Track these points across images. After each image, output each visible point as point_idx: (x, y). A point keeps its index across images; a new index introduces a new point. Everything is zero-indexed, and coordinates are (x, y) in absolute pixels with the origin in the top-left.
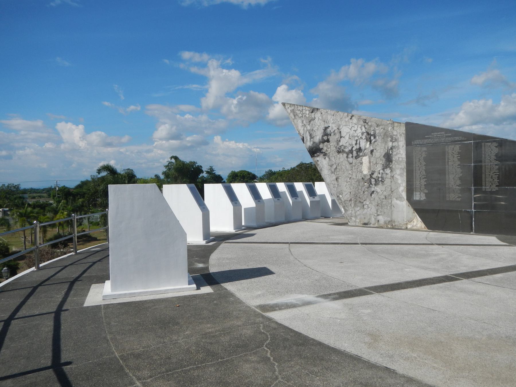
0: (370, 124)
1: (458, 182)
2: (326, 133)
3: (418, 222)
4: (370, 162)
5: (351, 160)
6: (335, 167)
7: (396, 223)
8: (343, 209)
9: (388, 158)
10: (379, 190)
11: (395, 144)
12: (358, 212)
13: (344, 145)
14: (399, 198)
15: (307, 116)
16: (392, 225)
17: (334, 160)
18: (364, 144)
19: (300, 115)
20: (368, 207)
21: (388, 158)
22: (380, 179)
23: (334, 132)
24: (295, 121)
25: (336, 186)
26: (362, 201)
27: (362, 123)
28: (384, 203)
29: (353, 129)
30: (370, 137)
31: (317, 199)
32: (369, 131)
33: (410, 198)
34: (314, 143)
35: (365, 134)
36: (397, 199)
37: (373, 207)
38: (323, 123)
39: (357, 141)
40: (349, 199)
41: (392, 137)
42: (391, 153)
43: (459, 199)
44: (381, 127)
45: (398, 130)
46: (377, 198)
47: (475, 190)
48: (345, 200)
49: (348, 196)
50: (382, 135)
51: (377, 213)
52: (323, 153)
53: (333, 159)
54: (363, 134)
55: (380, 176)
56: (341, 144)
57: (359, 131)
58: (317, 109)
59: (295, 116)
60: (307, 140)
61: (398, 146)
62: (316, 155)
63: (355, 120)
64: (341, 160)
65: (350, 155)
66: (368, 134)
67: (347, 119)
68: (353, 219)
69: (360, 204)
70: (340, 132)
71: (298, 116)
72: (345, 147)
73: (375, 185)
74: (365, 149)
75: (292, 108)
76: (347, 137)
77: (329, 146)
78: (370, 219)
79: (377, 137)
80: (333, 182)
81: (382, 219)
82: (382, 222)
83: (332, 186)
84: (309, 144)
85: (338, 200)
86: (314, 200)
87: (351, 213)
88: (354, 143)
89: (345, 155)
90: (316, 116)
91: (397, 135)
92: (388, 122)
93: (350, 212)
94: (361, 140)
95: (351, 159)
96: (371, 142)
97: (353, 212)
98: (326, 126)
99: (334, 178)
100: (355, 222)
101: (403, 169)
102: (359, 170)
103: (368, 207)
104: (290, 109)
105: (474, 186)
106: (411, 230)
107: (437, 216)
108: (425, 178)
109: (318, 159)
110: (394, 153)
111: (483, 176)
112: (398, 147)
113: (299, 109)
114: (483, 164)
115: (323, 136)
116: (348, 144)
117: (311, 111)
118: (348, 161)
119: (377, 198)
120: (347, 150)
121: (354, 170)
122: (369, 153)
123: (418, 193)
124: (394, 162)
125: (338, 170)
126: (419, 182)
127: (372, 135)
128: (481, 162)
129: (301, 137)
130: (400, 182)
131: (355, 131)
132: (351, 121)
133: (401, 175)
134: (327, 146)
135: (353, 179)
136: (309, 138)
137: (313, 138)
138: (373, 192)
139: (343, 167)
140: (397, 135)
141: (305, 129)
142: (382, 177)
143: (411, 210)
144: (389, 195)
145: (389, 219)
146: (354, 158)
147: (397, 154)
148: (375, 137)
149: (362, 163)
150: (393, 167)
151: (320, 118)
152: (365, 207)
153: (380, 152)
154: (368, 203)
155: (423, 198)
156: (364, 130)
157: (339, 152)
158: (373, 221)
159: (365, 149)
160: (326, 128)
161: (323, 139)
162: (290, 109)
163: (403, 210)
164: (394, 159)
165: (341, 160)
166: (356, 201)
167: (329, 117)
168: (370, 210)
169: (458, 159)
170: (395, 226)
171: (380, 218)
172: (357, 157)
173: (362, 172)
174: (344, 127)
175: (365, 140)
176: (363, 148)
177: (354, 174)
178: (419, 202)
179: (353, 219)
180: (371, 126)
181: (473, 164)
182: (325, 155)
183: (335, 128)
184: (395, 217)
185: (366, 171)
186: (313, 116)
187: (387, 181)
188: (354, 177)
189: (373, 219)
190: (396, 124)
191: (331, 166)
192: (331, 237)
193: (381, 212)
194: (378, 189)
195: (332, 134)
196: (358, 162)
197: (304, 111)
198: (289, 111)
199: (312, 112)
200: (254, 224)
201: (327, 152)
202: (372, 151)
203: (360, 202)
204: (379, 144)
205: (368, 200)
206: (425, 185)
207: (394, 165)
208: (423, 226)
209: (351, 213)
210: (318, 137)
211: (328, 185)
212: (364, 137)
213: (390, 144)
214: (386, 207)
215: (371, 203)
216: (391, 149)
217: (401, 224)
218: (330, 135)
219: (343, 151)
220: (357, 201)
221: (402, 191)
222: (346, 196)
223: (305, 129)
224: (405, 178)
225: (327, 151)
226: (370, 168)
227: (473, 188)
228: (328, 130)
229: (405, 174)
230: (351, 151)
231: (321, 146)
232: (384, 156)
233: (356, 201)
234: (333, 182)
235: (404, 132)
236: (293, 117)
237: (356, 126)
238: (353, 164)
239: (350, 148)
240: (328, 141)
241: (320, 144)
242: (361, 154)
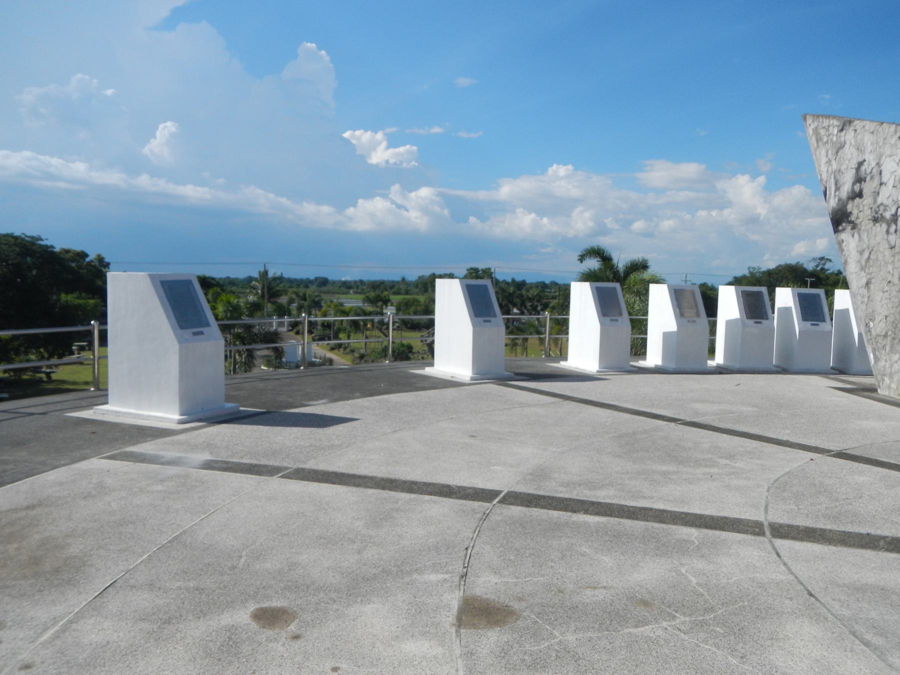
2: (859, 179)
6: (866, 255)
8: (871, 356)
13: (885, 202)
15: (835, 139)
17: (866, 240)
19: (825, 139)
25: (866, 300)
34: (840, 200)
38: (855, 153)
40: (884, 333)
49: (882, 325)
53: (864, 236)
56: (879, 201)
59: (817, 142)
60: (830, 194)
62: (840, 228)
75: (816, 124)
76: (890, 184)
84: (833, 203)
85: (866, 333)
97: (887, 366)
98: (861, 160)
99: (864, 281)
100: (889, 387)
104: (813, 126)
109: (843, 236)
113: (824, 125)
115: (854, 184)
116: (890, 199)
117: (840, 128)
118: (889, 242)
120: (888, 215)
125: (871, 262)
129: (823, 188)
134: (858, 206)
139: (880, 256)
151: (853, 141)
157: (875, 220)
160: (860, 164)
161: (853, 190)
166: (894, 339)
174: (888, 159)
179: (887, 380)
182: (854, 226)
183: (873, 164)
191: (861, 253)
195: (868, 179)
197: (831, 128)
198: (811, 132)
199: (842, 130)
200: (672, 366)
209: (885, 366)
211: (853, 296)
222: (879, 327)
228: (863, 168)
233: (894, 339)
240: (860, 195)
241: (847, 204)
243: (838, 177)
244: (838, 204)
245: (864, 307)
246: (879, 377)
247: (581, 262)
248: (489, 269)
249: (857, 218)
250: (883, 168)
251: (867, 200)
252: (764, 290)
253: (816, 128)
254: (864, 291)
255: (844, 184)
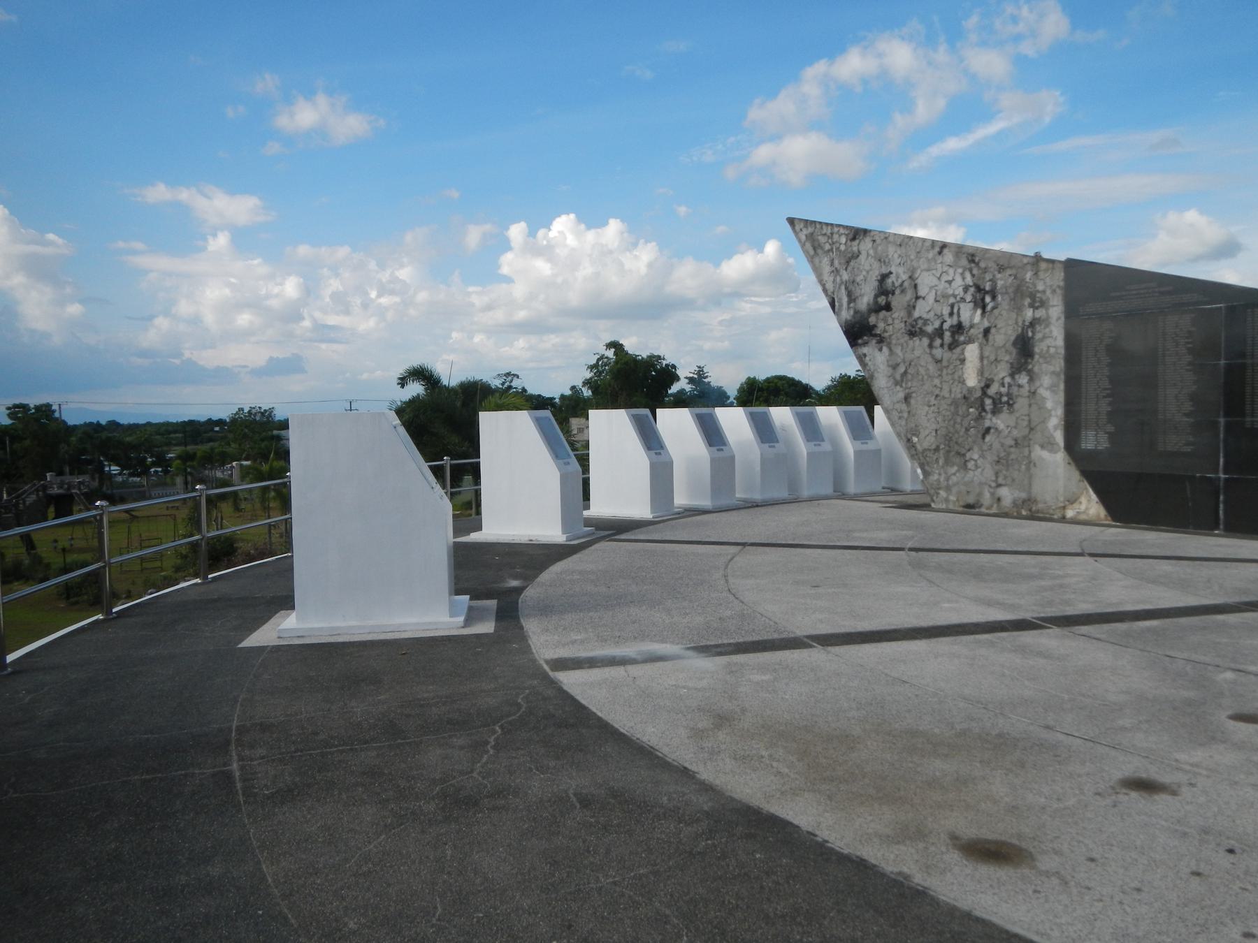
0: (982, 265)
1: (1188, 407)
2: (884, 290)
3: (1090, 505)
4: (982, 358)
5: (938, 352)
6: (902, 369)
7: (1041, 506)
9: (1024, 348)
10: (1001, 426)
11: (1040, 313)
12: (954, 479)
13: (925, 316)
14: (1048, 445)
15: (843, 248)
16: (1029, 511)
18: (969, 314)
19: (827, 247)
20: (977, 467)
21: (1024, 348)
22: (1005, 399)
23: (901, 285)
24: (817, 260)
25: (905, 415)
26: (963, 451)
27: (964, 262)
28: (1013, 456)
29: (945, 278)
30: (982, 296)
31: (871, 446)
32: (980, 283)
33: (1071, 446)
34: (856, 312)
35: (972, 290)
36: (1042, 447)
37: (988, 466)
38: (876, 265)
39: (952, 306)
40: (934, 447)
41: (1033, 296)
42: (1030, 334)
43: (1189, 449)
44: (1009, 272)
45: (1048, 280)
46: (996, 445)
47: (1228, 427)
48: (925, 450)
50: (1010, 290)
51: (996, 481)
52: (876, 335)
53: (898, 350)
54: (966, 289)
55: (1004, 390)
56: (916, 314)
57: (959, 281)
58: (865, 232)
59: (815, 249)
60: (841, 306)
61: (1048, 317)
63: (949, 257)
64: (917, 353)
65: (938, 342)
66: (979, 289)
67: (930, 255)
68: (943, 493)
69: (957, 460)
70: (916, 286)
71: (822, 248)
72: (926, 322)
73: (996, 411)
74: (972, 326)
75: (810, 230)
77: (890, 321)
78: (980, 494)
79: (999, 298)
80: (897, 406)
81: (1008, 495)
82: (1007, 501)
83: (895, 414)
84: (846, 315)
86: (864, 447)
87: (938, 480)
88: (946, 311)
89: (926, 341)
90: (862, 247)
91: (1044, 292)
92: (1025, 261)
93: (936, 477)
94: (962, 305)
95: (940, 350)
96: (984, 307)
98: (884, 270)
99: (901, 395)
100: (947, 500)
101: (1058, 375)
102: (956, 377)
103: (977, 467)
104: (805, 232)
105: (1227, 415)
106: (1075, 522)
107: (1138, 492)
108: (1108, 396)
109: (865, 350)
110: (1038, 336)
111: (1248, 390)
112: (1046, 321)
114: (1249, 361)
115: (876, 296)
116: (932, 314)
117: (851, 236)
118: (933, 356)
119: (996, 445)
120: (929, 329)
121: (945, 378)
122: (981, 336)
123: (1091, 434)
124: (1037, 357)
125: (909, 377)
126: (1096, 405)
127: (987, 292)
128: (1243, 355)
130: (1049, 405)
131: (950, 282)
132: (940, 259)
133: (1052, 388)
134: (885, 320)
135: (944, 398)
136: (845, 300)
137: (854, 300)
138: (988, 430)
139: (922, 371)
140: (1044, 292)
141: (838, 279)
142: (1008, 394)
143: (1076, 475)
144: (1025, 437)
145: (1024, 495)
146: (946, 347)
147: (1044, 338)
148: (994, 298)
149: (963, 361)
150: (1036, 369)
151: (871, 252)
152: (971, 465)
153: (1004, 335)
154: (976, 456)
155: (1104, 444)
156: (969, 280)
157: (912, 334)
158: (987, 498)
159: (972, 326)
160: (884, 277)
161: (876, 302)
162: (805, 232)
163: (1054, 471)
164: (1037, 350)
165: (917, 353)
166: (949, 452)
167: (891, 249)
168: (981, 472)
169: (1188, 349)
170: (1038, 511)
171: (1004, 492)
172: (953, 346)
173: (963, 382)
174: (925, 274)
175: (971, 305)
176: (966, 323)
177: (946, 387)
178: (1092, 455)
179: (943, 493)
180: (985, 270)
181: (1222, 362)
182: (881, 340)
183: (904, 277)
184: (1037, 490)
185: (972, 381)
186: (855, 249)
187: (1021, 404)
188: (945, 393)
189: (987, 495)
190: (1043, 265)
191: (895, 367)
192: (857, 534)
193: (1005, 477)
194: (1000, 422)
195: (897, 292)
196: (955, 357)
197: (836, 237)
198: (803, 238)
199: (854, 239)
200: (706, 503)
201: (886, 335)
202: (987, 332)
203: (958, 453)
204: (1004, 313)
205: (976, 449)
206: (1109, 413)
207: (1038, 365)
208: (1102, 512)
209: (938, 480)
210: (866, 297)
212: (969, 298)
213: (1029, 314)
214: (1016, 467)
215: (982, 456)
216: (1032, 325)
217: (1049, 507)
218: (893, 294)
219: (922, 333)
220: (952, 449)
221: (1056, 428)
223: (838, 279)
224: (1061, 397)
225: (885, 331)
226: (981, 372)
227: (1222, 420)
228: (889, 281)
229: (1062, 386)
230: (939, 332)
231: (872, 320)
232: (1015, 344)
233: (949, 452)
234: (897, 406)
235: (1062, 284)
236: (812, 252)
237: (951, 271)
238: (945, 363)
239: (937, 324)
240: (888, 307)
242: (962, 338)
243: (851, 287)
244: (854, 316)
245: (903, 423)
246: (932, 492)
247: (403, 386)
248: (48, 406)
249: (885, 331)
250: (919, 281)
251: (898, 314)
252: (862, 409)
253: (812, 234)
254: (904, 407)
255: (862, 295)
